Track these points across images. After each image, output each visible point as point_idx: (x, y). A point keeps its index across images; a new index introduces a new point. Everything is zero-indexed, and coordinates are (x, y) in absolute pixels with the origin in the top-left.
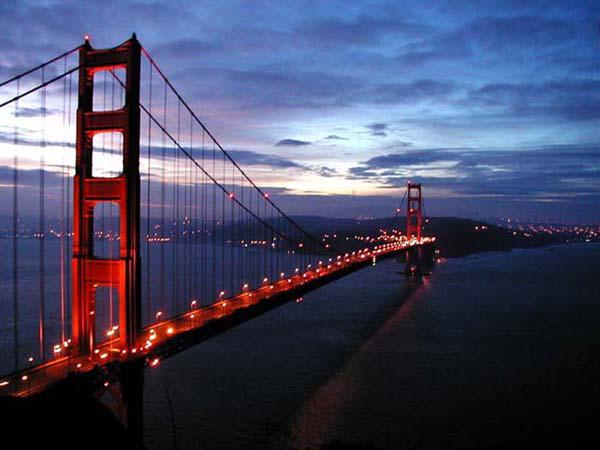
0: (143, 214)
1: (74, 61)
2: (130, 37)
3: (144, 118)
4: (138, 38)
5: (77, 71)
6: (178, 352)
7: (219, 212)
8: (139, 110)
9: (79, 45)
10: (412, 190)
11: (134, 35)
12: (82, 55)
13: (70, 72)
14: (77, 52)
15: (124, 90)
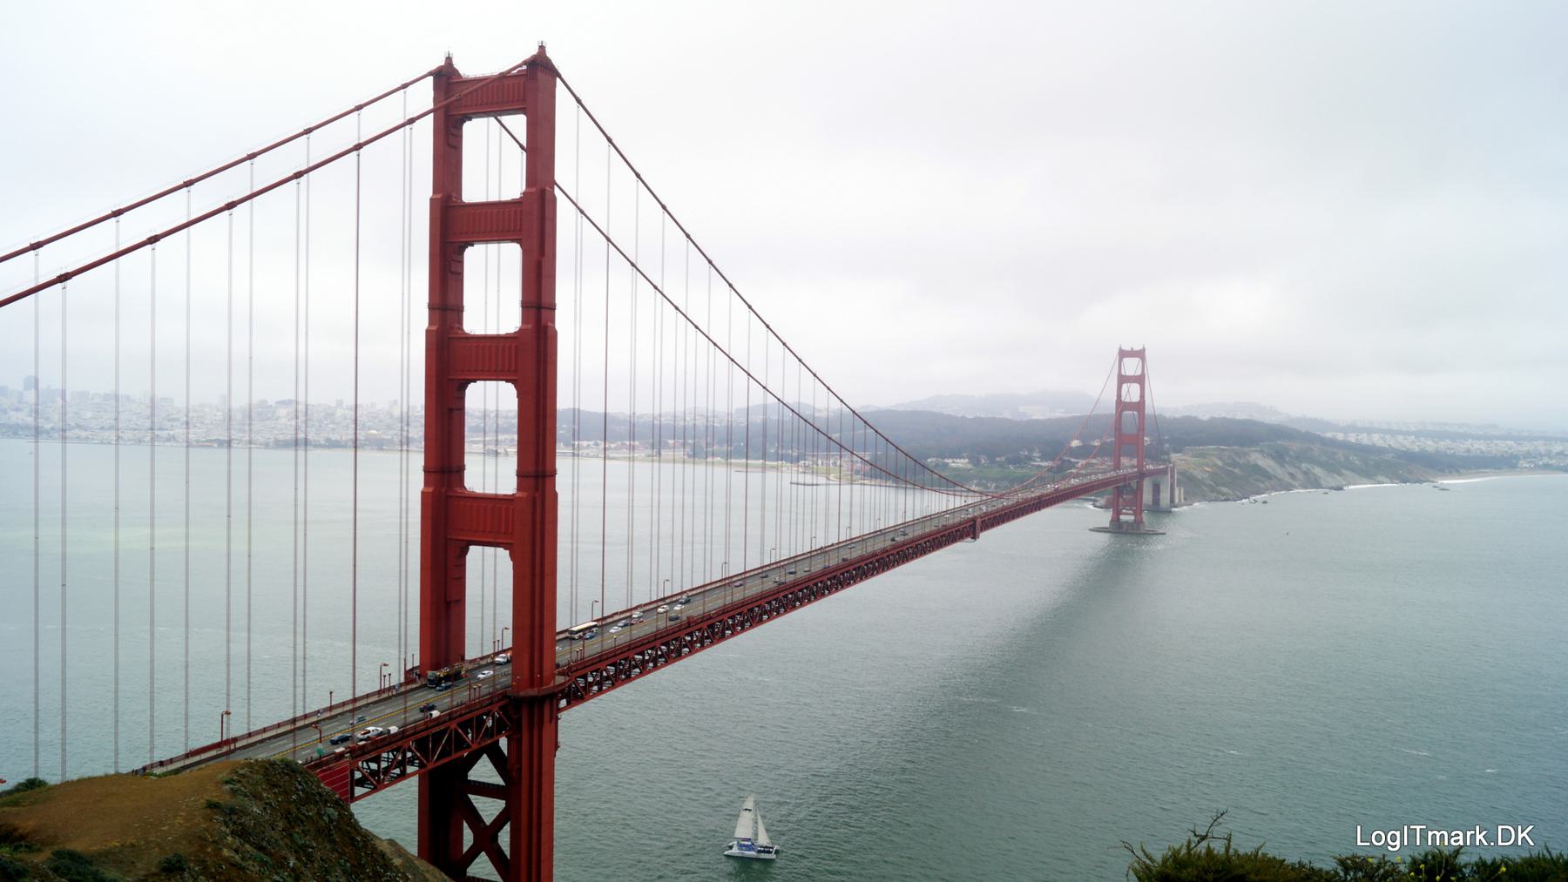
0: (564, 400)
1: (424, 96)
2: (534, 51)
3: (564, 214)
4: (549, 54)
5: (432, 114)
6: (629, 678)
7: (690, 405)
8: (554, 199)
9: (433, 66)
10: (1126, 360)
11: (542, 48)
12: (436, 88)
13: (411, 121)
14: (431, 79)
15: (525, 153)
